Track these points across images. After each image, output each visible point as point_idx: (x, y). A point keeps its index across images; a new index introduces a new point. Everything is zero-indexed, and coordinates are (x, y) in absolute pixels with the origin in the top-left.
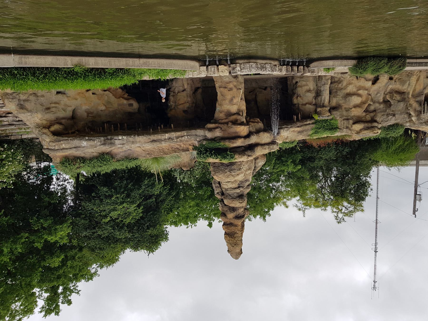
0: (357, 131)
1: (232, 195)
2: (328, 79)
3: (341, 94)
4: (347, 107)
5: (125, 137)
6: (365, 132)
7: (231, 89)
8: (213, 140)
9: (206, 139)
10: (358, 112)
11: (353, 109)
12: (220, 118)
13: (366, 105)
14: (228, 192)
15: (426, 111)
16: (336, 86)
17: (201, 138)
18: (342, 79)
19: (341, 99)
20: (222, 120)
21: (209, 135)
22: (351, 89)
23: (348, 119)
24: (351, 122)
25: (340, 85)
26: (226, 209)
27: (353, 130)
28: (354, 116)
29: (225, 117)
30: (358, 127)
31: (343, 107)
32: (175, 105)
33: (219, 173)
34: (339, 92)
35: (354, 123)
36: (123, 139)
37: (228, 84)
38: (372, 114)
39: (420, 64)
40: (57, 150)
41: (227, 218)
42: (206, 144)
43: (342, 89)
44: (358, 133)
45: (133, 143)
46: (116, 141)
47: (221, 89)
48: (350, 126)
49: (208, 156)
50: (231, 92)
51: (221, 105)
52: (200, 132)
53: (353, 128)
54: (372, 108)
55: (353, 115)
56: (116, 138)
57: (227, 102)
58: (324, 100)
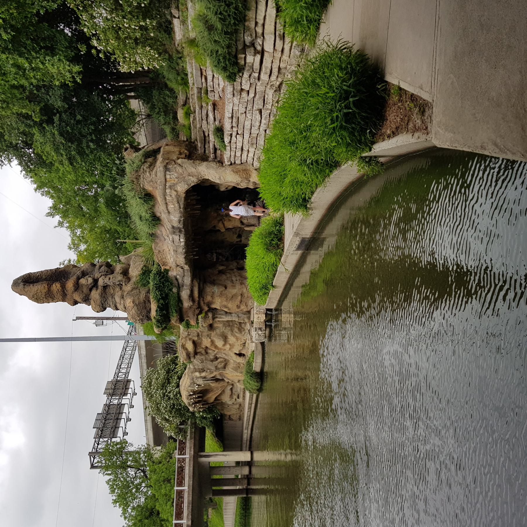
0: (185, 345)
1: (106, 302)
2: (244, 320)
3: (227, 331)
4: (212, 335)
5: (183, 244)
6: (184, 354)
7: (238, 307)
8: (179, 300)
9: (179, 287)
10: (206, 342)
11: (209, 340)
12: (205, 298)
13: (214, 349)
14: (110, 299)
15: (205, 382)
16: (236, 326)
17: (180, 281)
18: (243, 333)
19: (222, 331)
20: (203, 300)
21: (185, 294)
22: (231, 339)
23: (198, 336)
24: (196, 339)
25: (236, 330)
26: (85, 290)
27: (186, 340)
28: (202, 340)
29: (206, 301)
30: (190, 346)
31: (212, 333)
32: (223, 216)
33: (137, 311)
34: (229, 328)
35: (194, 342)
36: (181, 242)
37: (244, 304)
38: (203, 352)
39: (250, 404)
40: (165, 199)
41: (73, 293)
42: (173, 293)
43: (232, 331)
44: (183, 347)
45: (176, 251)
46: (178, 237)
47: (239, 297)
48: (190, 337)
49: (158, 301)
50: (235, 307)
51: (221, 295)
52: (187, 280)
53: (188, 342)
54: (210, 351)
55: (204, 339)
56: (182, 236)
57: (225, 303)
58: (221, 318)
